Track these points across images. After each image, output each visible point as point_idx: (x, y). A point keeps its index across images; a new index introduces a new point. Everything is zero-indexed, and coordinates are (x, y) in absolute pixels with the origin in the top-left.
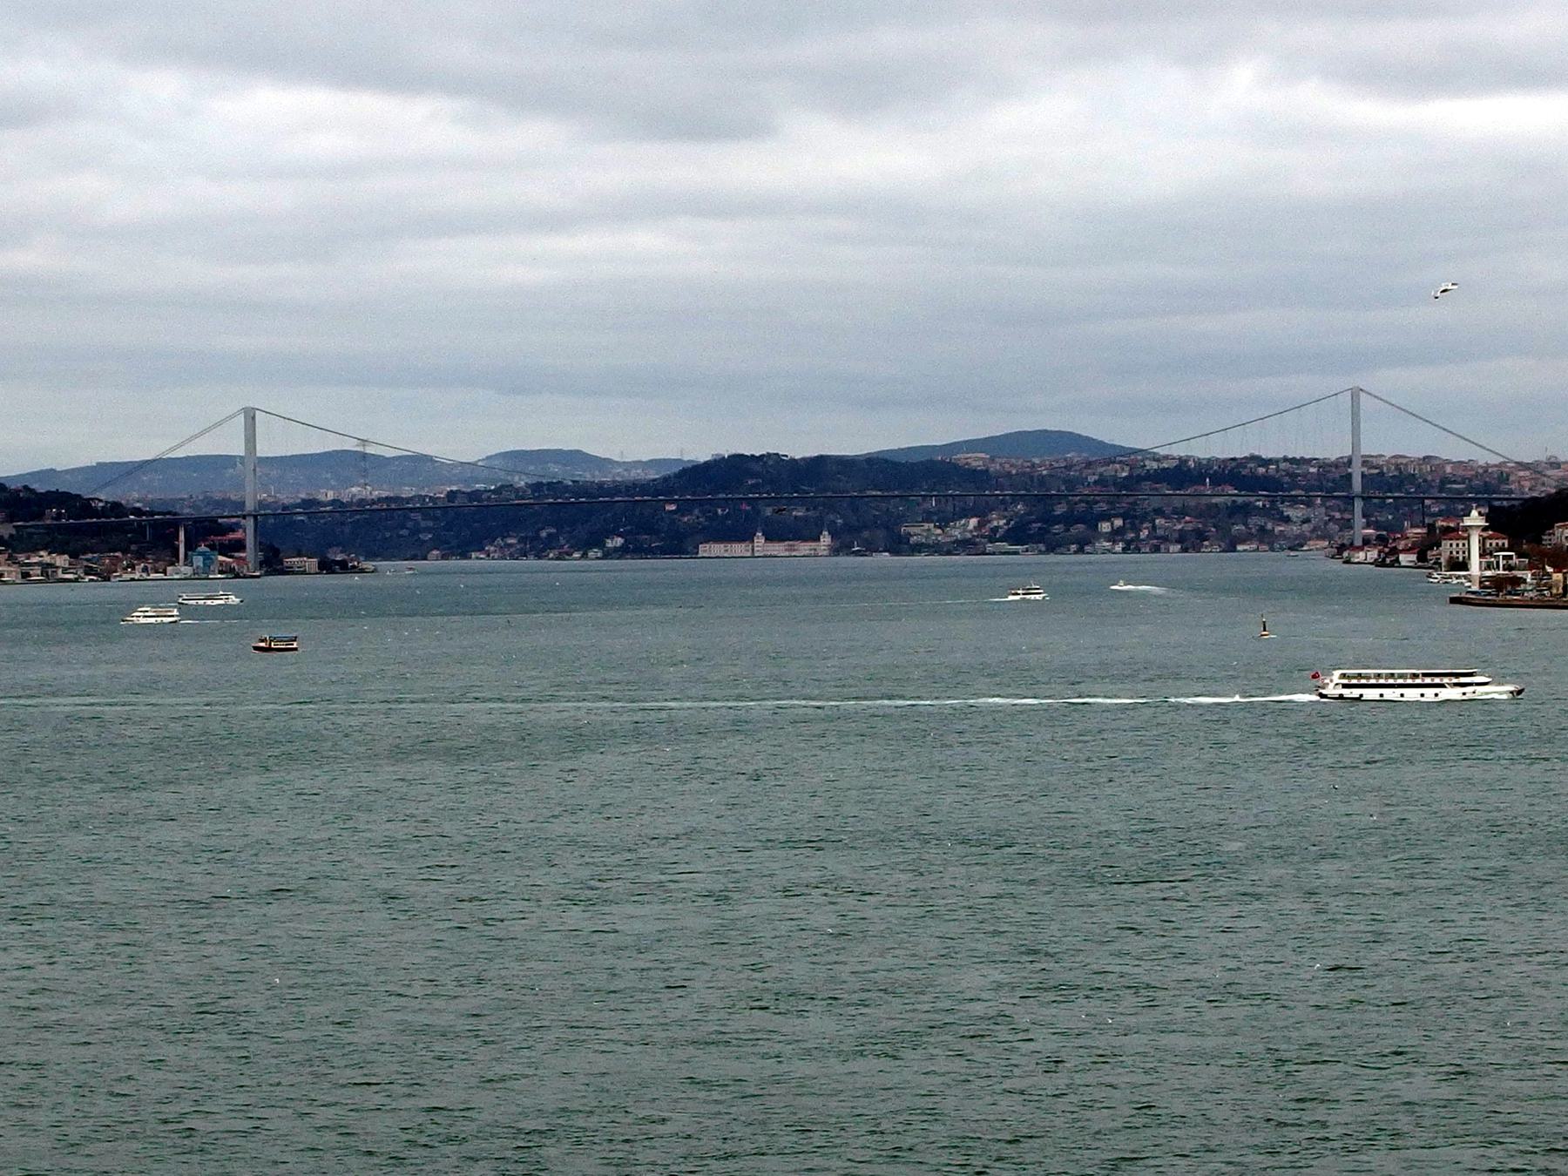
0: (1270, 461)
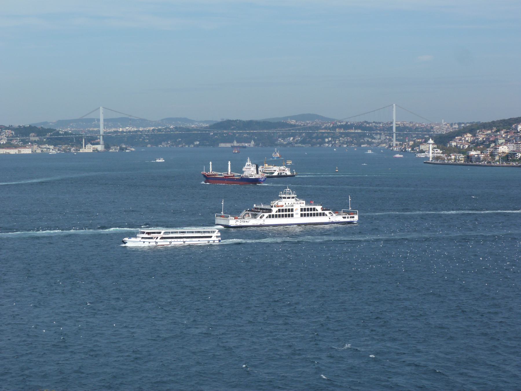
0: (370, 123)
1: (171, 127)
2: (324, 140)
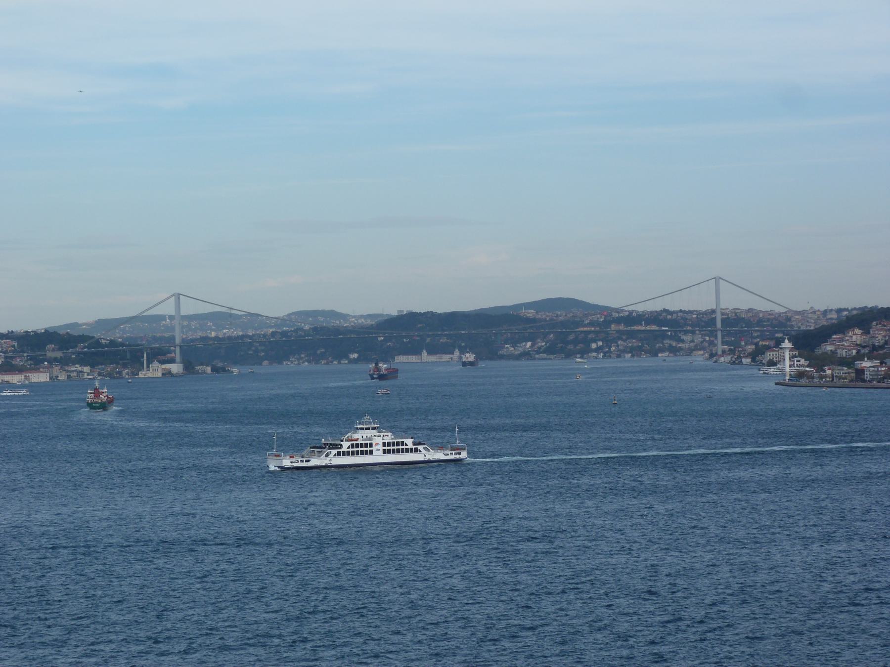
0: (674, 312)
1: (307, 327)
2: (589, 346)
